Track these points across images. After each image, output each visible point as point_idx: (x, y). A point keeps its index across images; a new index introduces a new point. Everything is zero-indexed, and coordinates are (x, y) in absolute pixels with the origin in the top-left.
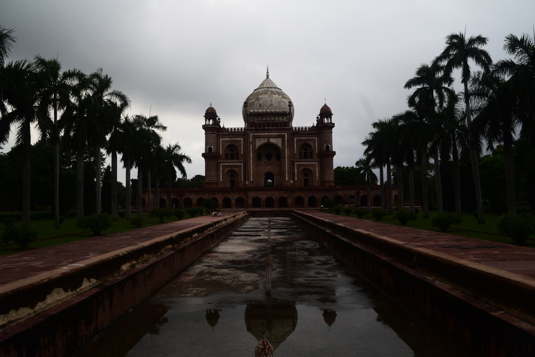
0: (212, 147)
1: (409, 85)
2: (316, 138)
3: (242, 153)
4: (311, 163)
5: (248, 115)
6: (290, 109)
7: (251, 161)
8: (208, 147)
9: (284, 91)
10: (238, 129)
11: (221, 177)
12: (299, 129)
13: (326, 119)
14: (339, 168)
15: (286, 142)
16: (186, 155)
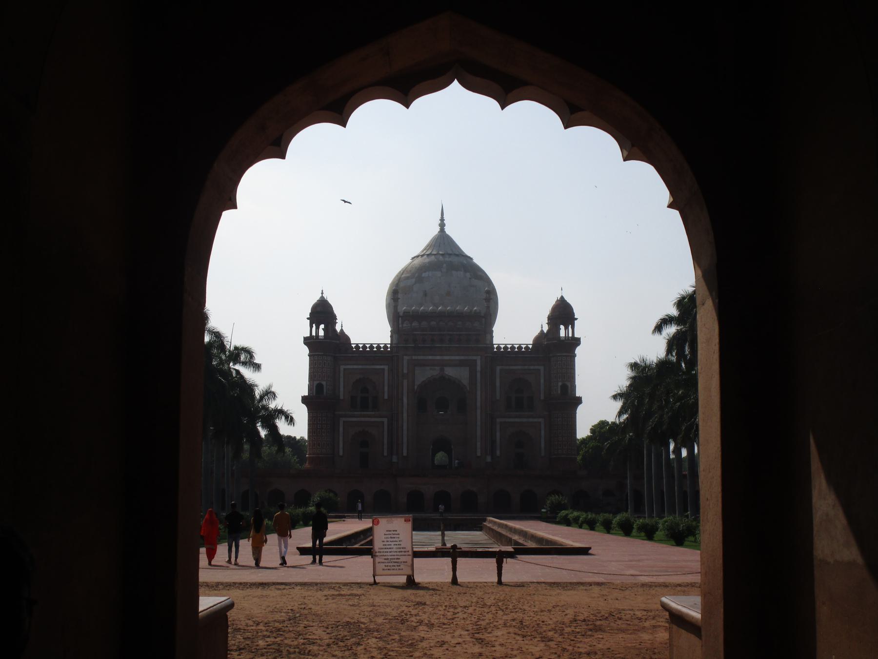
0: (324, 383)
1: (659, 328)
2: (542, 368)
3: (386, 397)
4: (531, 420)
5: (399, 316)
6: (488, 307)
7: (405, 415)
8: (316, 383)
9: (477, 261)
10: (378, 347)
11: (341, 446)
12: (506, 348)
13: (562, 327)
14: (603, 424)
15: (479, 375)
16: (285, 409)
